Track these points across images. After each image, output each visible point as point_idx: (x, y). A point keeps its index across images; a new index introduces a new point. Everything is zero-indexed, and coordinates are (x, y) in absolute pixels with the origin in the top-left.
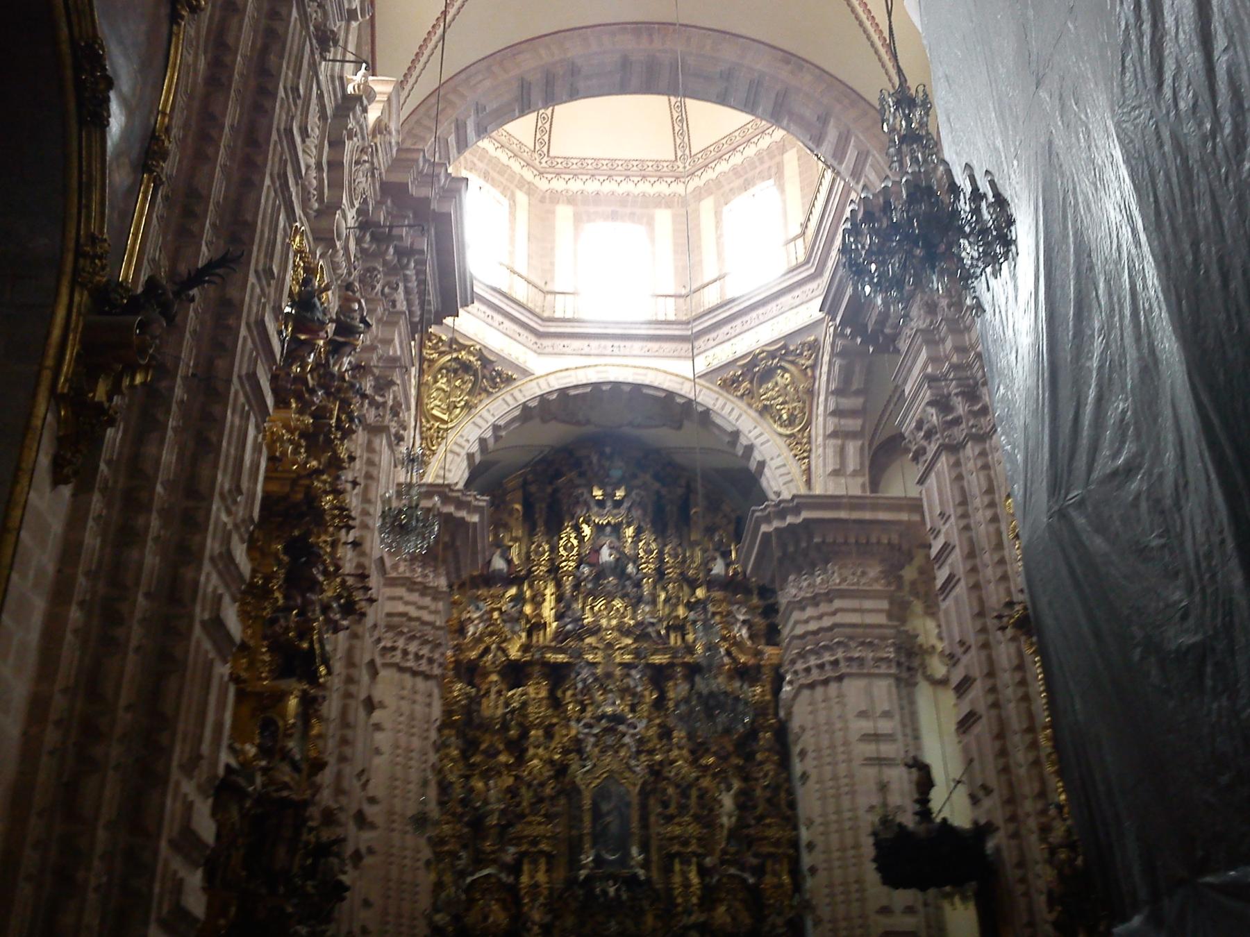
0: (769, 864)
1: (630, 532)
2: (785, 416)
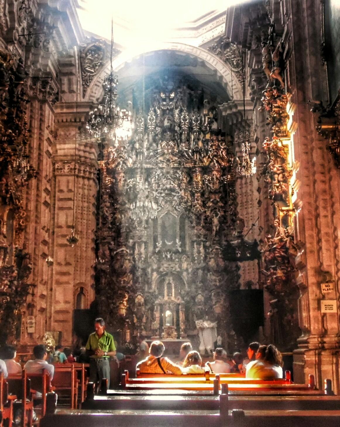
1: (177, 112)
2: (235, 63)
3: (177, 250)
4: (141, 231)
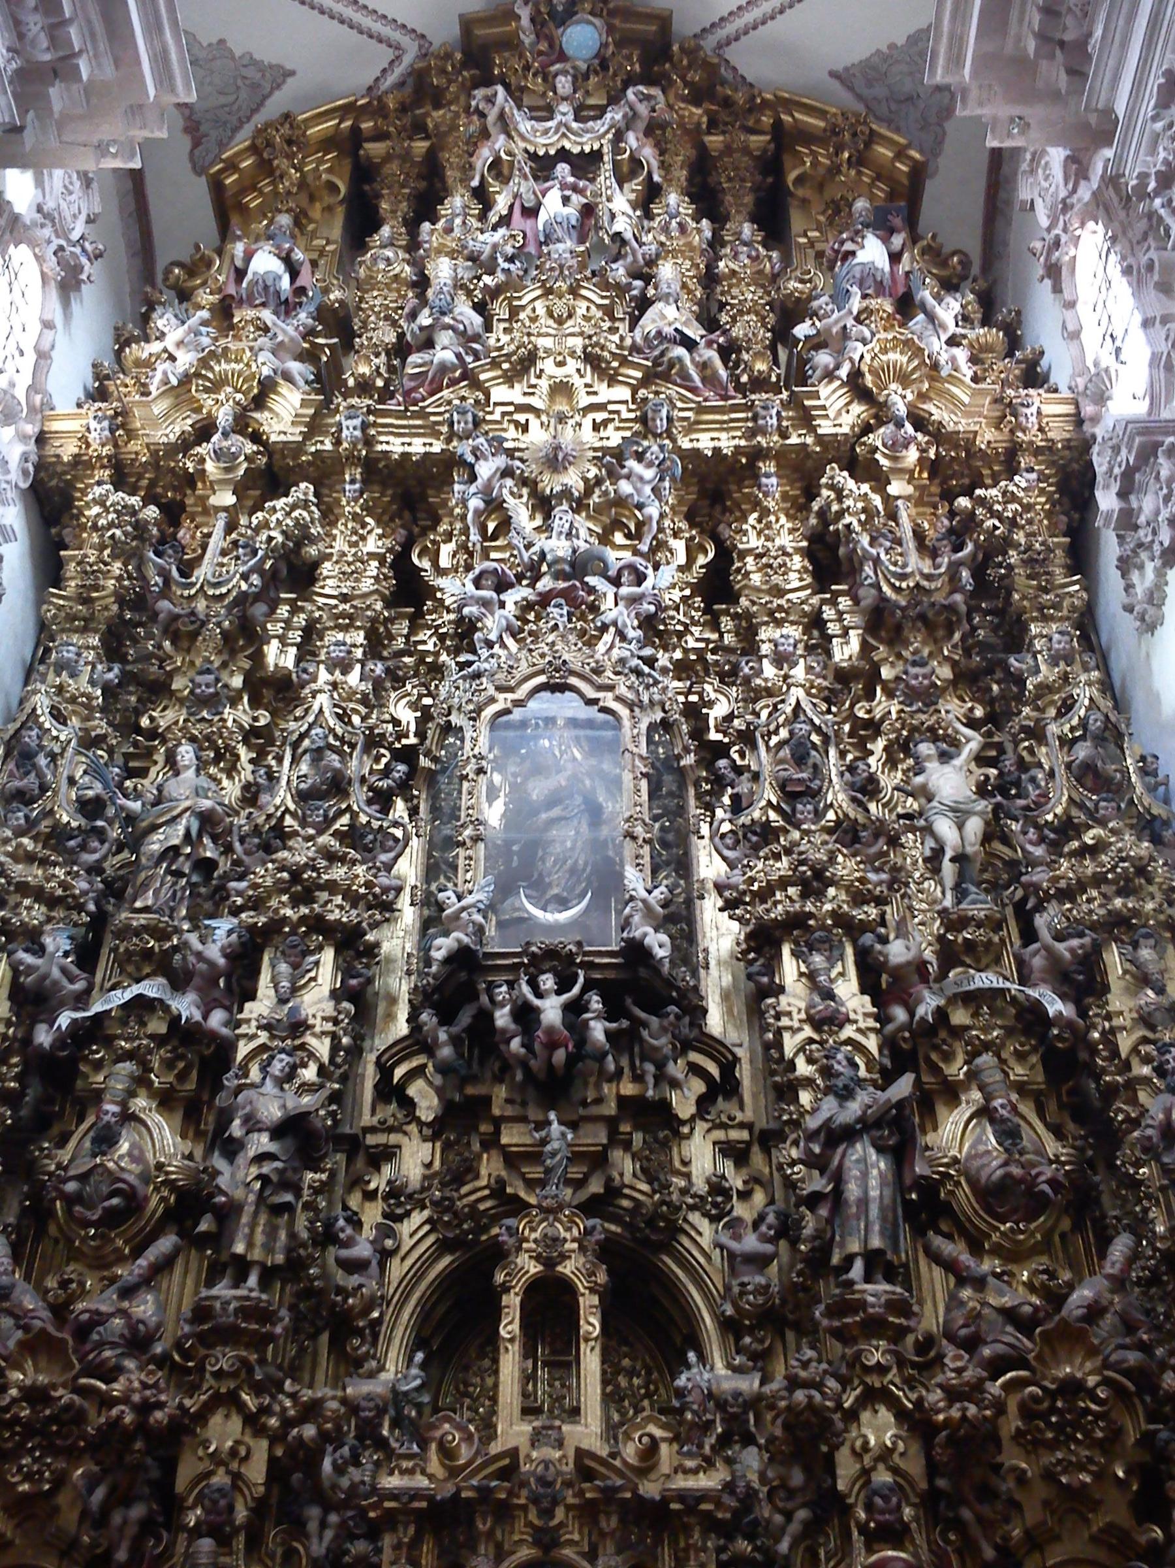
0: (1114, 959)
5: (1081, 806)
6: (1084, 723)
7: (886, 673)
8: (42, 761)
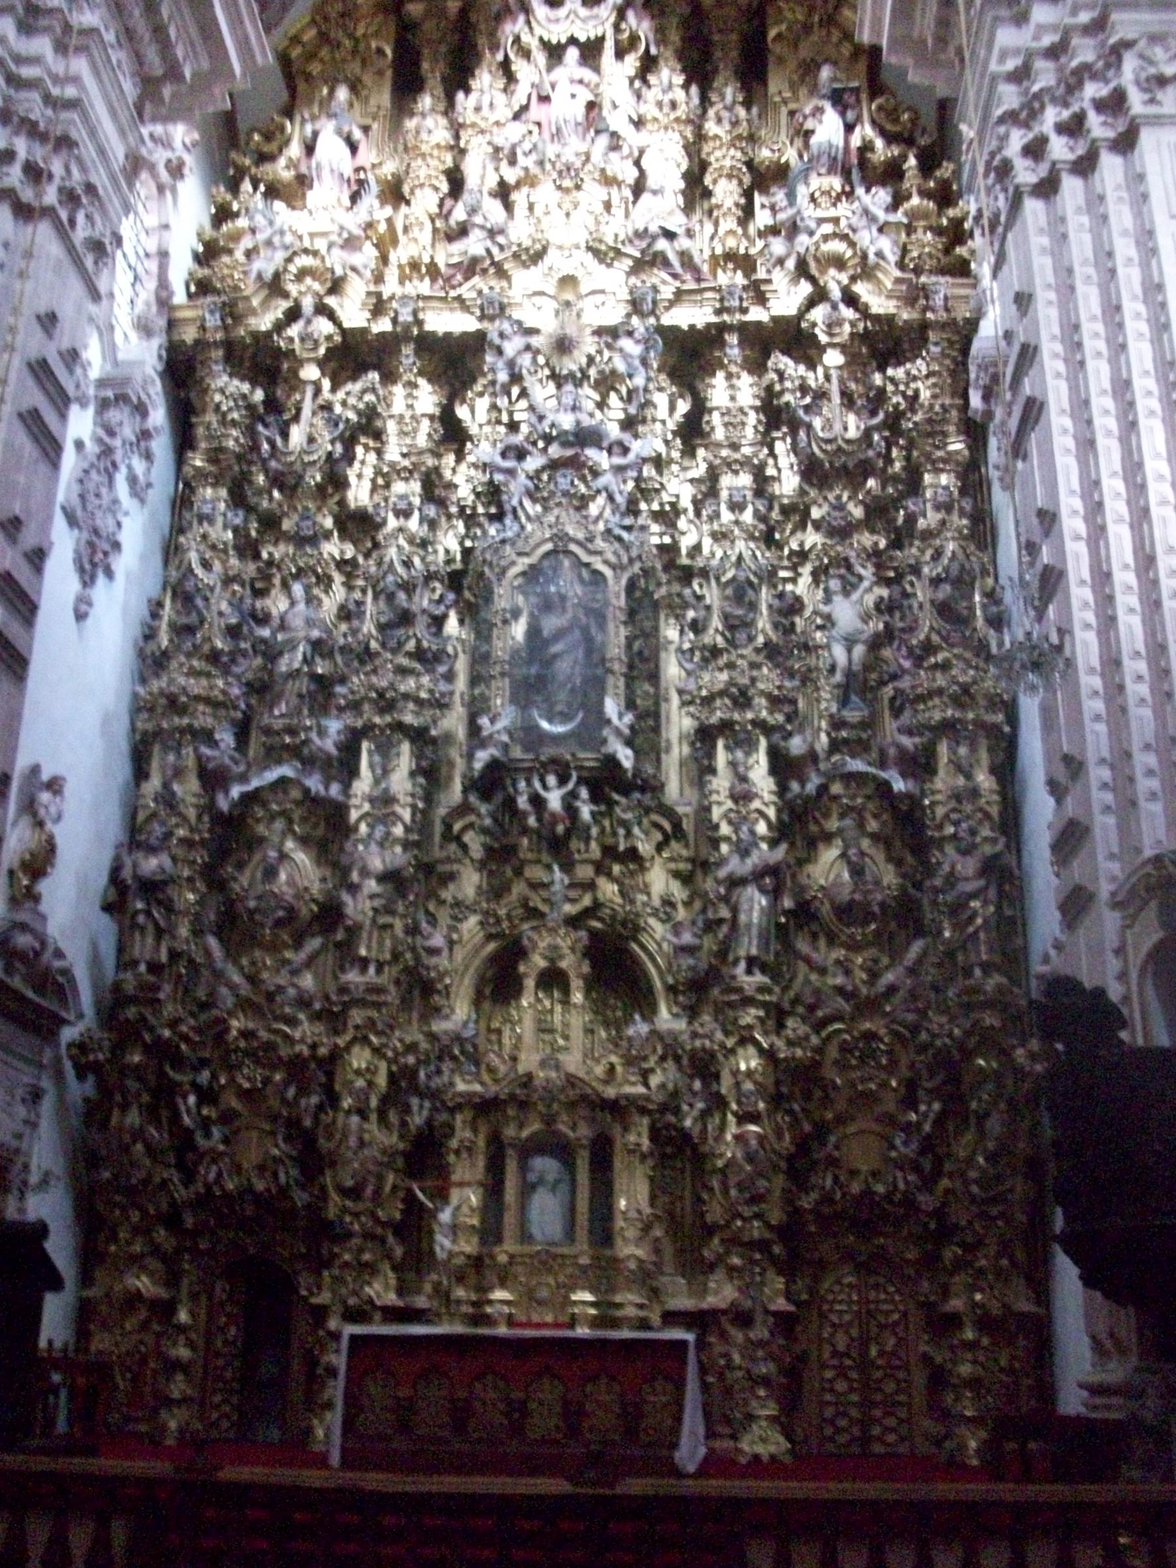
3: (612, 762)
4: (403, 671)
5: (939, 633)
6: (946, 570)
7: (816, 513)
8: (199, 602)
